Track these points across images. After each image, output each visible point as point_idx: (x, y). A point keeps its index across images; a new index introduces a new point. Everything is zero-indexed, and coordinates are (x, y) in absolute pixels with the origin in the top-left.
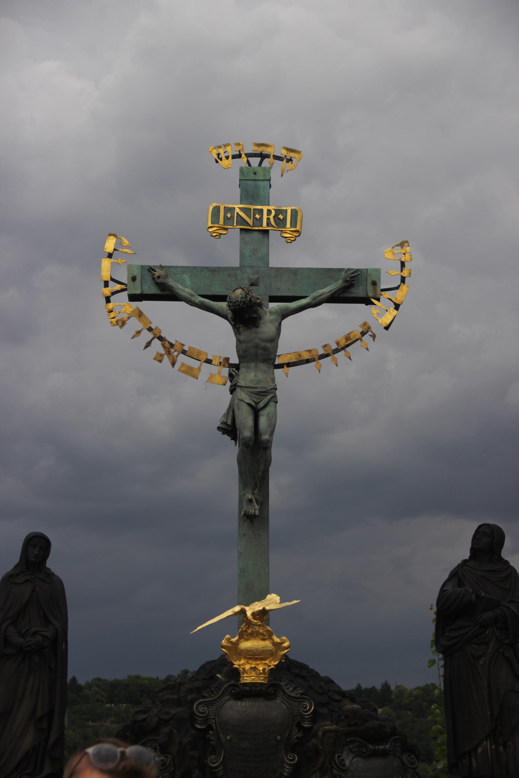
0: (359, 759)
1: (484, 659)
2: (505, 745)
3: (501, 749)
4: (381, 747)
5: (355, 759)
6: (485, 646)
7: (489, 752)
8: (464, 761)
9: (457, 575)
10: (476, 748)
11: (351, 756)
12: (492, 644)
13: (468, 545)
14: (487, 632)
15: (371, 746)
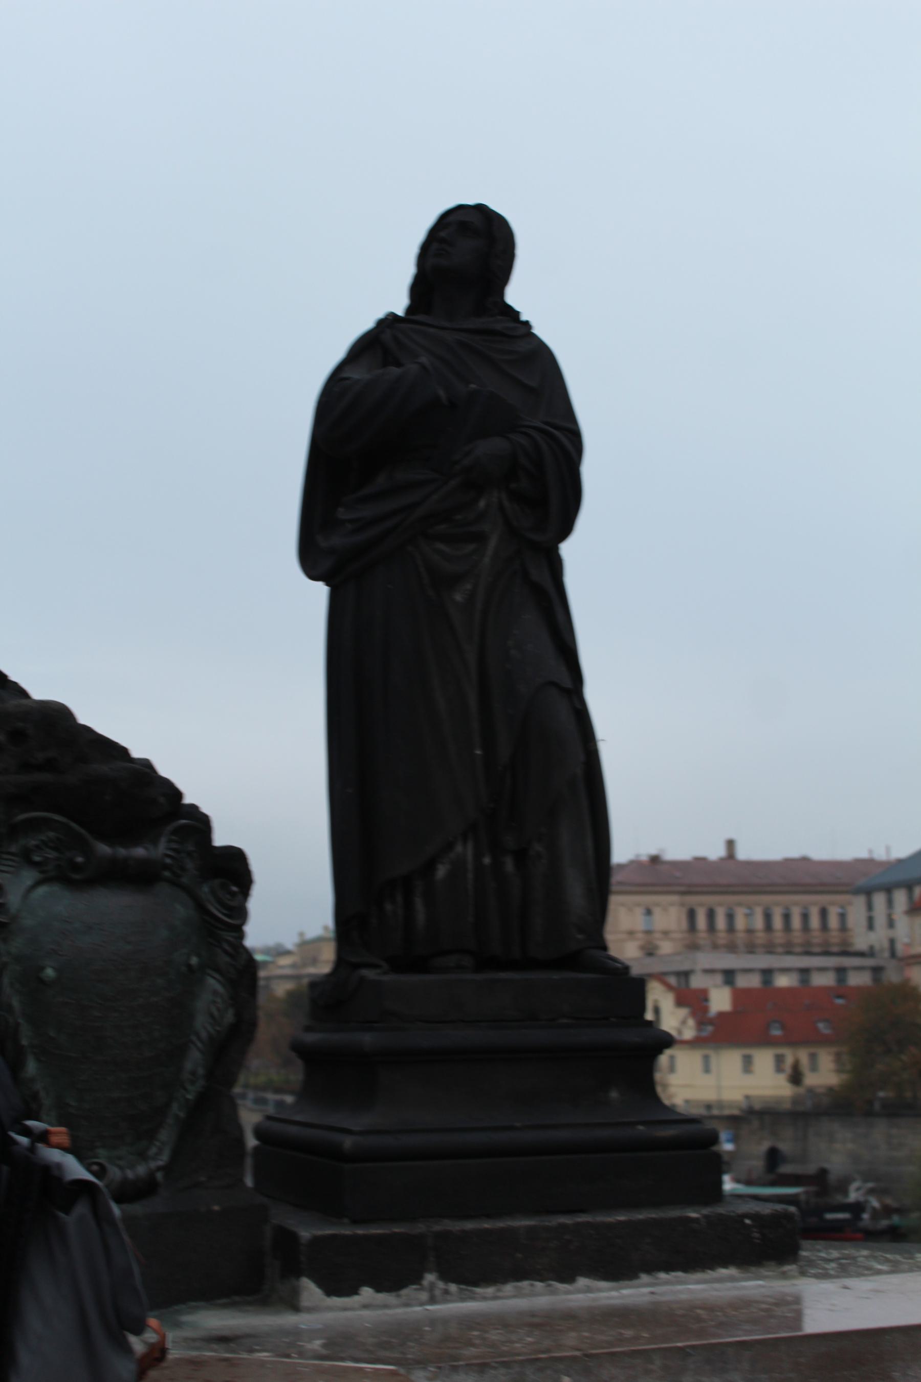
0: (55, 889)
1: (469, 586)
2: (521, 856)
3: (509, 865)
4: (139, 852)
5: (42, 890)
6: (471, 547)
7: (470, 876)
8: (388, 907)
9: (378, 345)
10: (430, 866)
11: (29, 876)
12: (493, 543)
13: (405, 270)
14: (482, 504)
15: (104, 849)
